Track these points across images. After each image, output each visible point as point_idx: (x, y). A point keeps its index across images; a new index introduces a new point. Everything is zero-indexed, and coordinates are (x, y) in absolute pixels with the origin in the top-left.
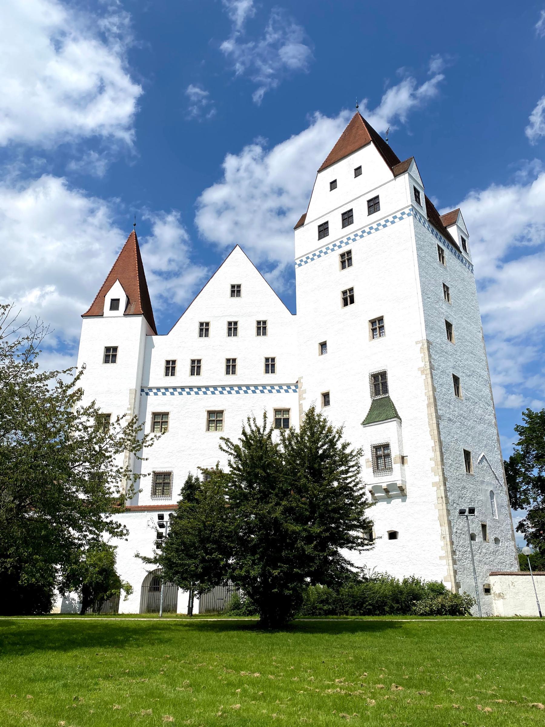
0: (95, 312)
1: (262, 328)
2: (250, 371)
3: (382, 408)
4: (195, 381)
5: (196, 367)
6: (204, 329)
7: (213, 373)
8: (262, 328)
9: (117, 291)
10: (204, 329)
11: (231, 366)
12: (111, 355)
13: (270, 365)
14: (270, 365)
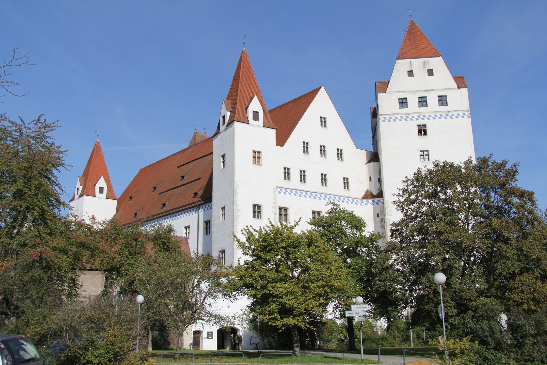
6: (306, 147)
11: (324, 179)
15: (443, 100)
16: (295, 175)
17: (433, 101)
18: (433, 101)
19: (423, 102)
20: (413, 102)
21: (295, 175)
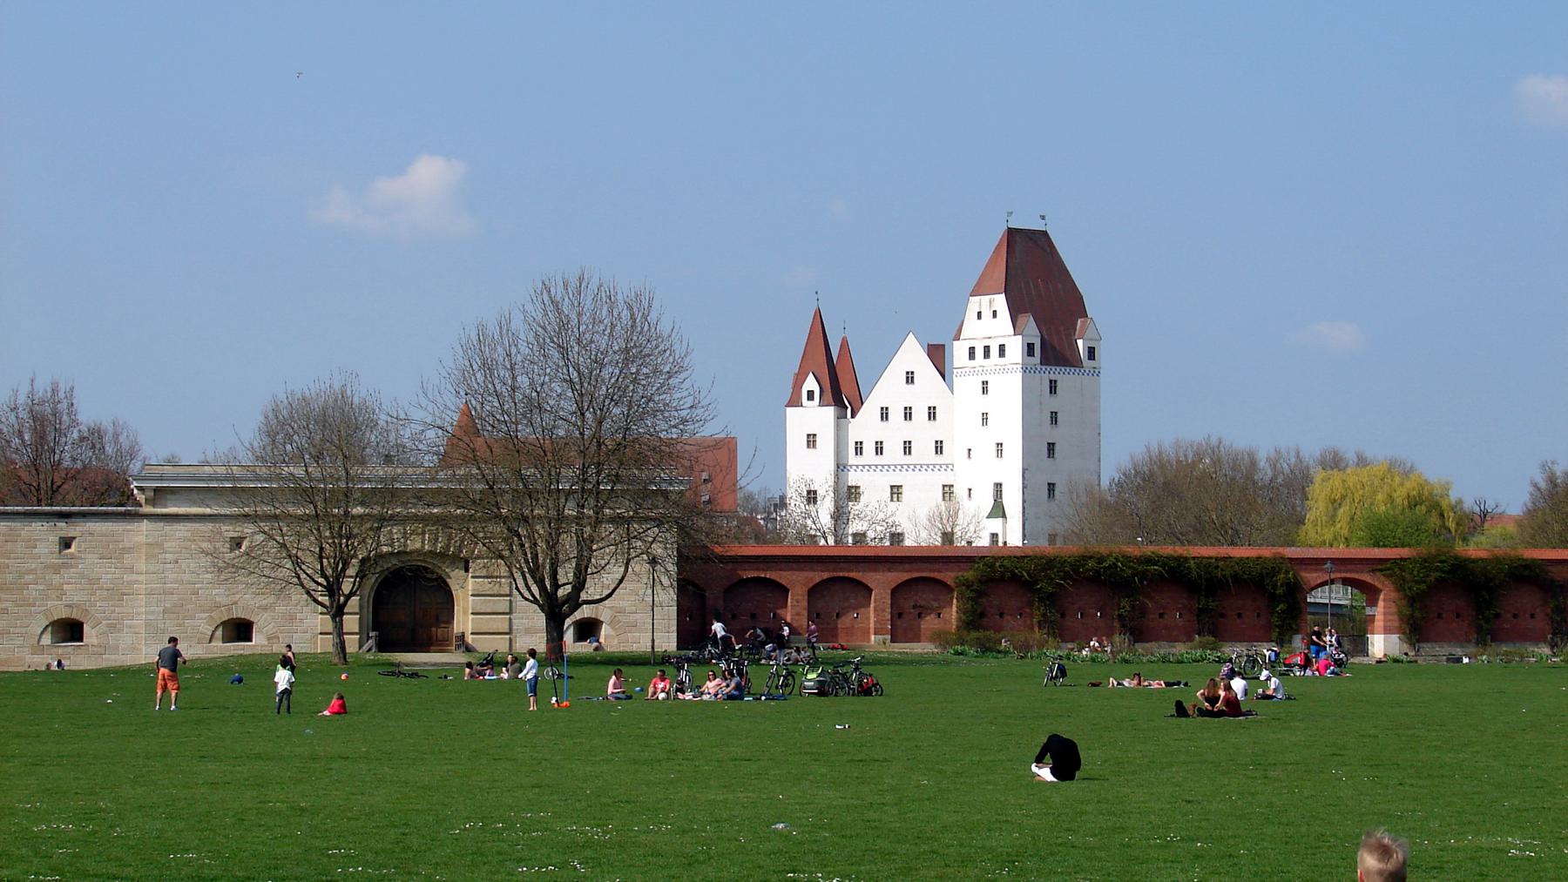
0: (795, 402)
1: (932, 414)
2: (922, 451)
3: (998, 511)
4: (879, 460)
5: (879, 449)
6: (885, 414)
7: (893, 452)
8: (932, 414)
9: (811, 384)
10: (885, 414)
11: (907, 448)
12: (811, 440)
13: (939, 448)
14: (939, 448)
15: (1002, 349)
16: (869, 448)
17: (994, 351)
18: (994, 351)
19: (987, 350)
20: (979, 353)
21: (869, 448)
